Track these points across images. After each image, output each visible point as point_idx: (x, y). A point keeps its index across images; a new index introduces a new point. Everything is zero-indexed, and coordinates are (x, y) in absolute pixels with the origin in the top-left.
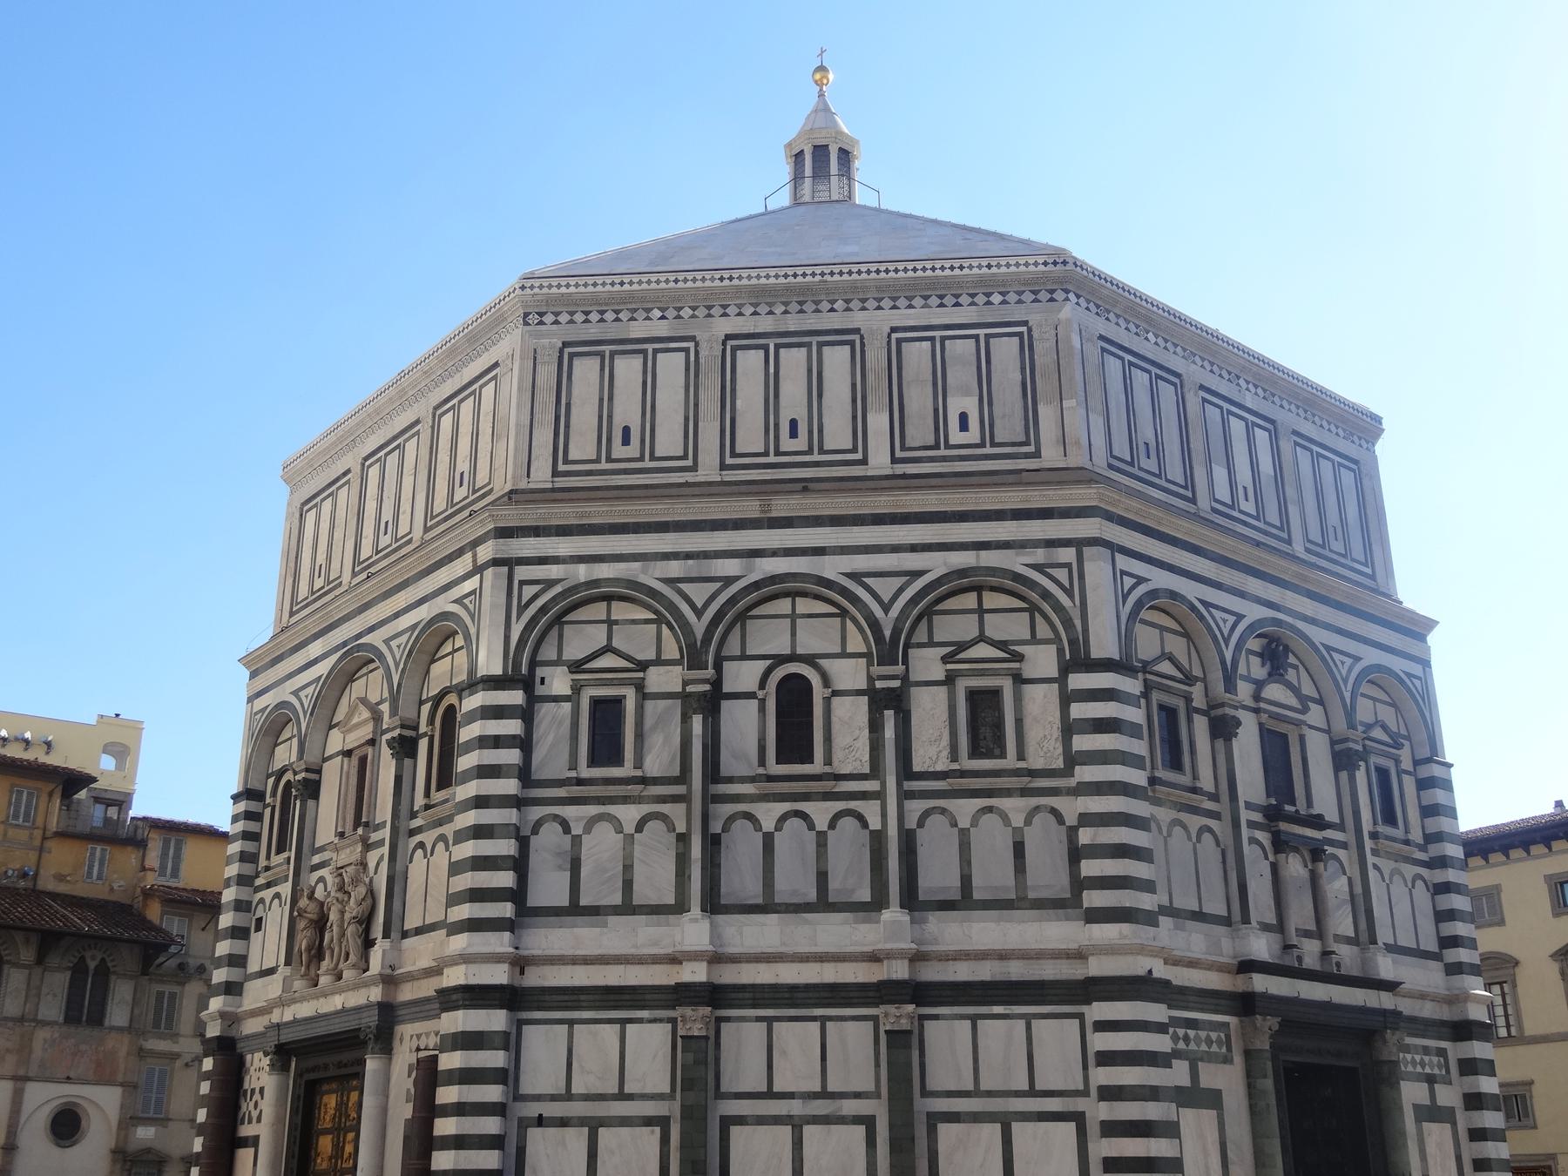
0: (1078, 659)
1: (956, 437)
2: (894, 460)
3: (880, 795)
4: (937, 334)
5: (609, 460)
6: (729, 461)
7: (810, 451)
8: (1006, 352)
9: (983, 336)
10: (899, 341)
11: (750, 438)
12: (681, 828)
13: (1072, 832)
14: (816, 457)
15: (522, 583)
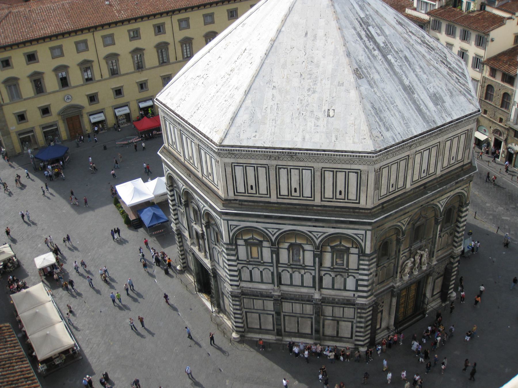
0: (362, 253)
1: (338, 196)
2: (322, 201)
3: (315, 270)
4: (335, 170)
5: (248, 193)
6: (279, 196)
7: (300, 196)
8: (353, 177)
9: (347, 173)
10: (324, 171)
11: (284, 191)
12: (272, 270)
13: (357, 281)
14: (301, 198)
15: (231, 225)
